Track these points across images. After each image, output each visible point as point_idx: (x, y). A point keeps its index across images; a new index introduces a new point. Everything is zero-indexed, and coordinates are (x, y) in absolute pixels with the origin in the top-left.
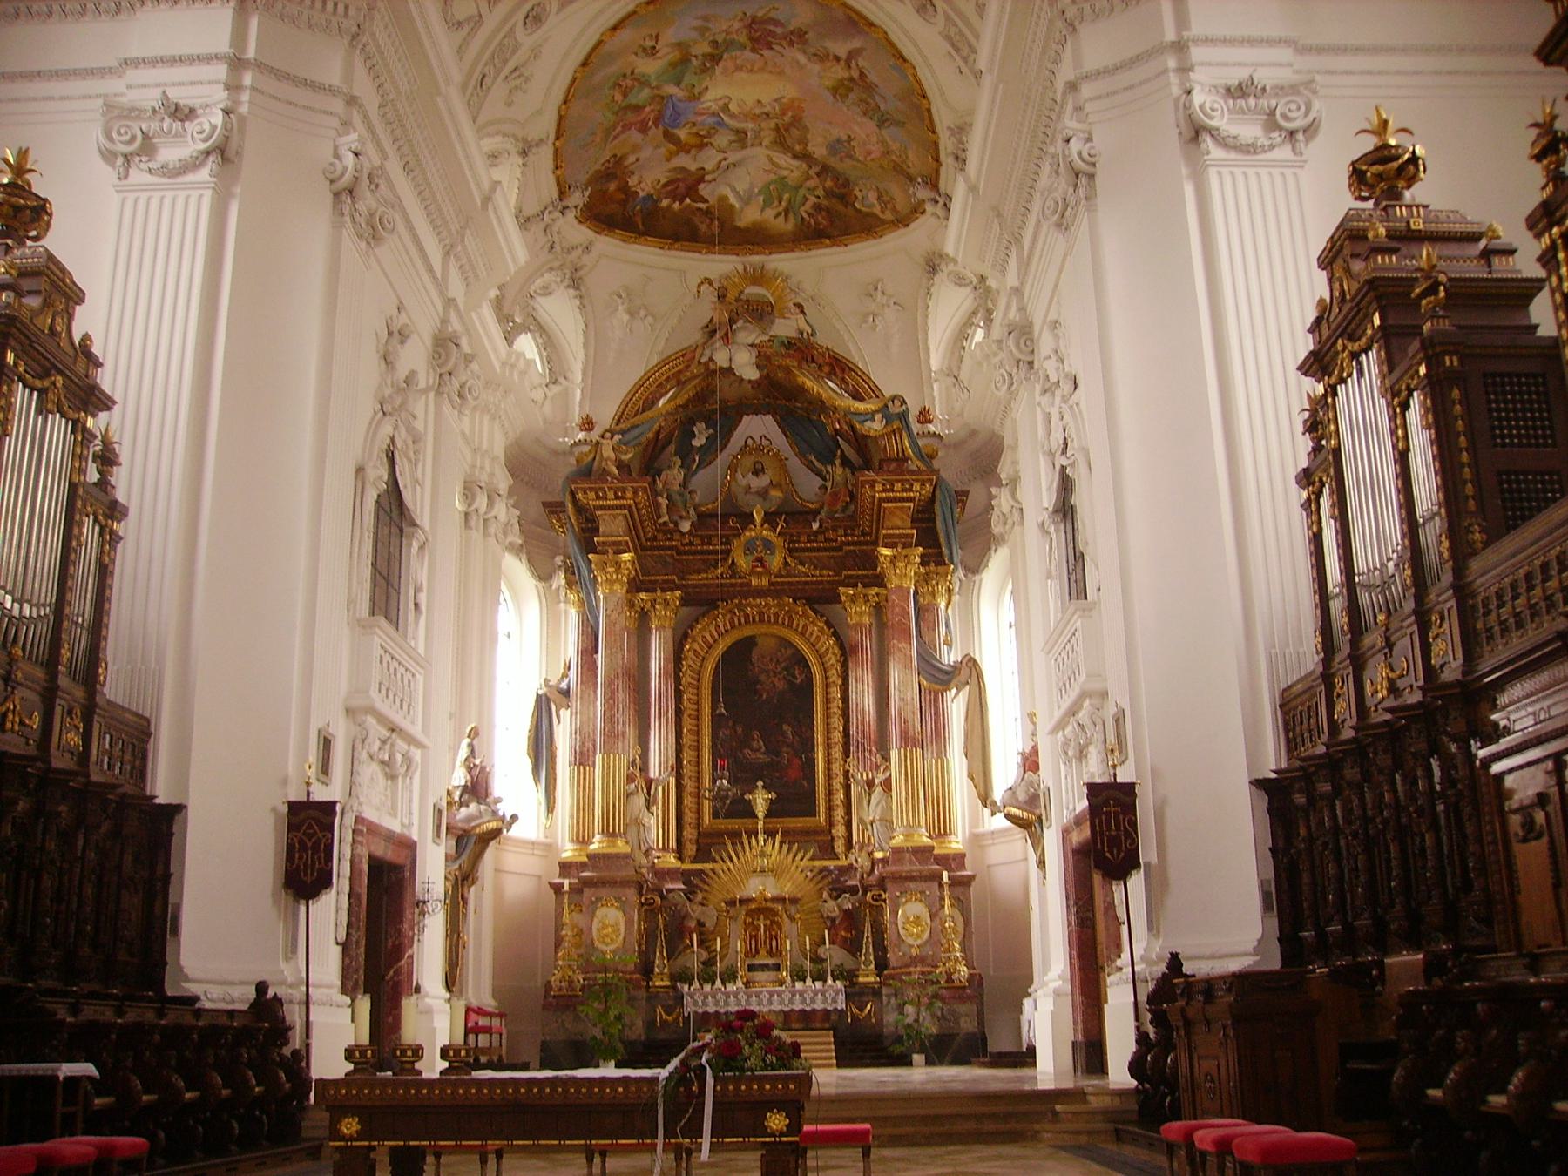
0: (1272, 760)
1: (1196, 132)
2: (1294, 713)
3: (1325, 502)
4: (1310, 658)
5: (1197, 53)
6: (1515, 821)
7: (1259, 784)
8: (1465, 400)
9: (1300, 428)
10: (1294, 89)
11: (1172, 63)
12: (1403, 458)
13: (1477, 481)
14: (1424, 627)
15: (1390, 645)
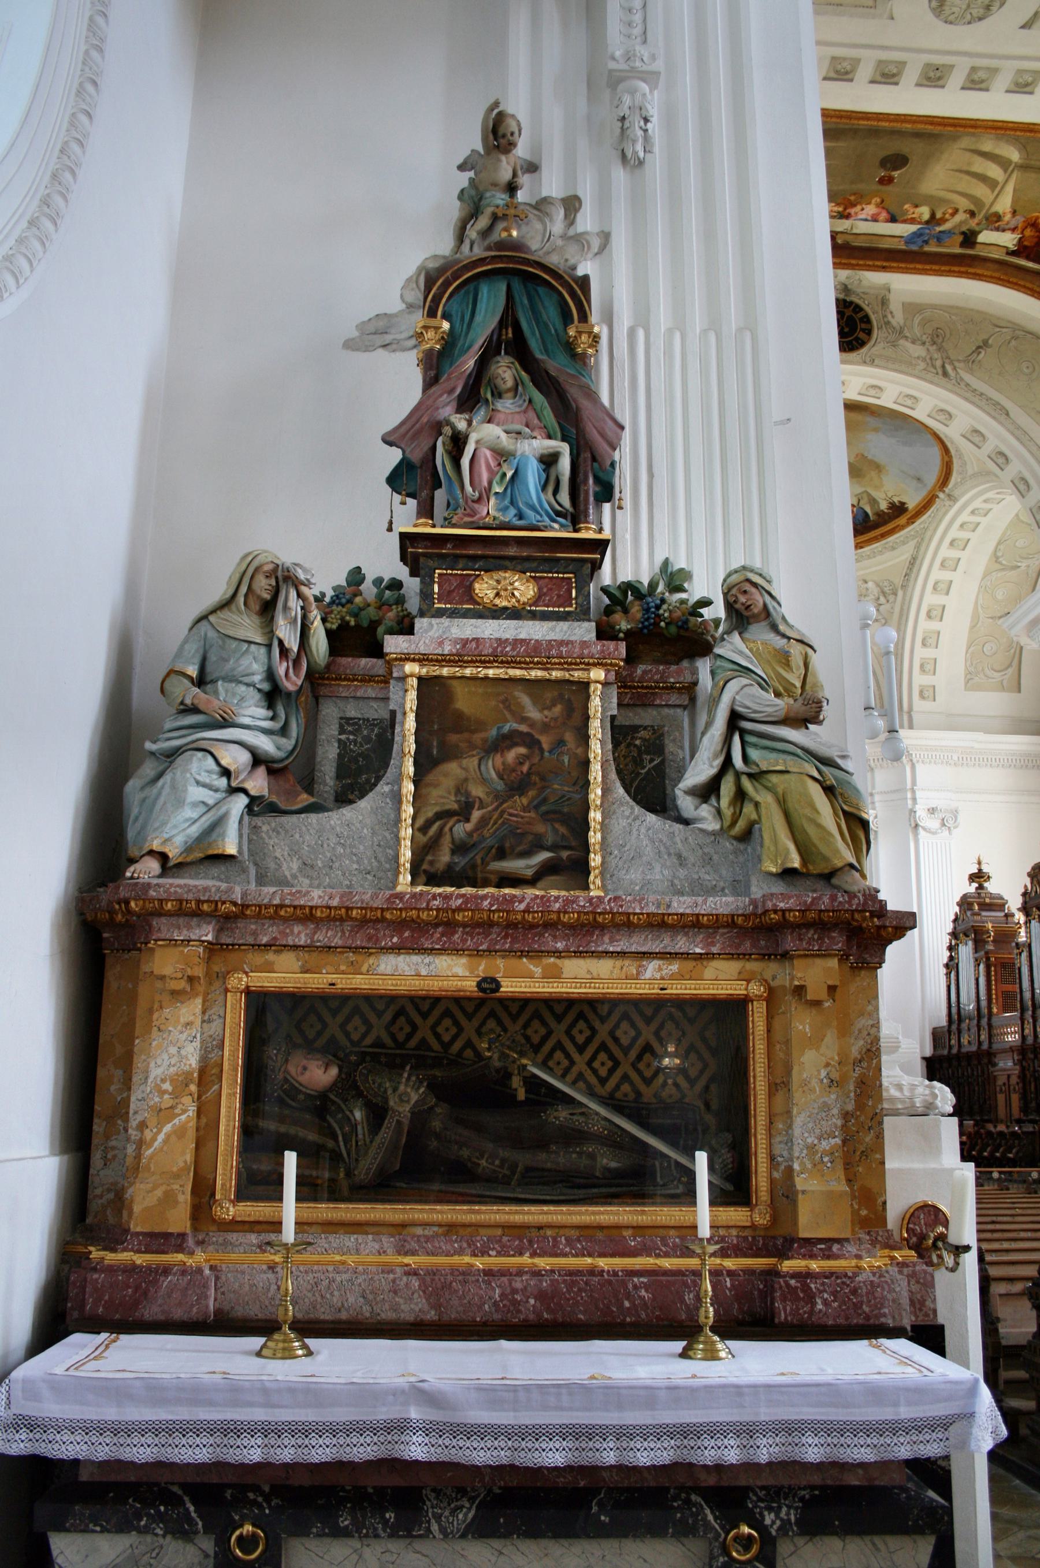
0: (928, 1052)
1: (917, 825)
2: (937, 1036)
3: (953, 974)
4: (943, 1022)
5: (918, 794)
6: (998, 1089)
7: (924, 1058)
8: (995, 971)
9: (945, 948)
10: (951, 812)
11: (909, 795)
12: (977, 980)
13: (996, 994)
14: (979, 1030)
15: (969, 1029)
